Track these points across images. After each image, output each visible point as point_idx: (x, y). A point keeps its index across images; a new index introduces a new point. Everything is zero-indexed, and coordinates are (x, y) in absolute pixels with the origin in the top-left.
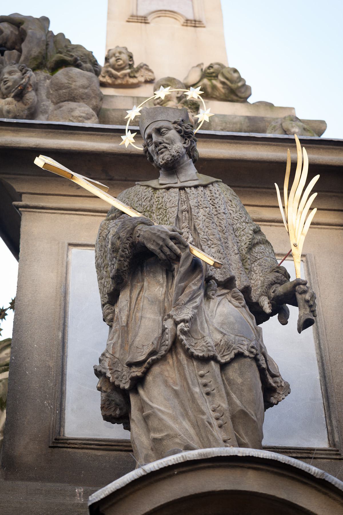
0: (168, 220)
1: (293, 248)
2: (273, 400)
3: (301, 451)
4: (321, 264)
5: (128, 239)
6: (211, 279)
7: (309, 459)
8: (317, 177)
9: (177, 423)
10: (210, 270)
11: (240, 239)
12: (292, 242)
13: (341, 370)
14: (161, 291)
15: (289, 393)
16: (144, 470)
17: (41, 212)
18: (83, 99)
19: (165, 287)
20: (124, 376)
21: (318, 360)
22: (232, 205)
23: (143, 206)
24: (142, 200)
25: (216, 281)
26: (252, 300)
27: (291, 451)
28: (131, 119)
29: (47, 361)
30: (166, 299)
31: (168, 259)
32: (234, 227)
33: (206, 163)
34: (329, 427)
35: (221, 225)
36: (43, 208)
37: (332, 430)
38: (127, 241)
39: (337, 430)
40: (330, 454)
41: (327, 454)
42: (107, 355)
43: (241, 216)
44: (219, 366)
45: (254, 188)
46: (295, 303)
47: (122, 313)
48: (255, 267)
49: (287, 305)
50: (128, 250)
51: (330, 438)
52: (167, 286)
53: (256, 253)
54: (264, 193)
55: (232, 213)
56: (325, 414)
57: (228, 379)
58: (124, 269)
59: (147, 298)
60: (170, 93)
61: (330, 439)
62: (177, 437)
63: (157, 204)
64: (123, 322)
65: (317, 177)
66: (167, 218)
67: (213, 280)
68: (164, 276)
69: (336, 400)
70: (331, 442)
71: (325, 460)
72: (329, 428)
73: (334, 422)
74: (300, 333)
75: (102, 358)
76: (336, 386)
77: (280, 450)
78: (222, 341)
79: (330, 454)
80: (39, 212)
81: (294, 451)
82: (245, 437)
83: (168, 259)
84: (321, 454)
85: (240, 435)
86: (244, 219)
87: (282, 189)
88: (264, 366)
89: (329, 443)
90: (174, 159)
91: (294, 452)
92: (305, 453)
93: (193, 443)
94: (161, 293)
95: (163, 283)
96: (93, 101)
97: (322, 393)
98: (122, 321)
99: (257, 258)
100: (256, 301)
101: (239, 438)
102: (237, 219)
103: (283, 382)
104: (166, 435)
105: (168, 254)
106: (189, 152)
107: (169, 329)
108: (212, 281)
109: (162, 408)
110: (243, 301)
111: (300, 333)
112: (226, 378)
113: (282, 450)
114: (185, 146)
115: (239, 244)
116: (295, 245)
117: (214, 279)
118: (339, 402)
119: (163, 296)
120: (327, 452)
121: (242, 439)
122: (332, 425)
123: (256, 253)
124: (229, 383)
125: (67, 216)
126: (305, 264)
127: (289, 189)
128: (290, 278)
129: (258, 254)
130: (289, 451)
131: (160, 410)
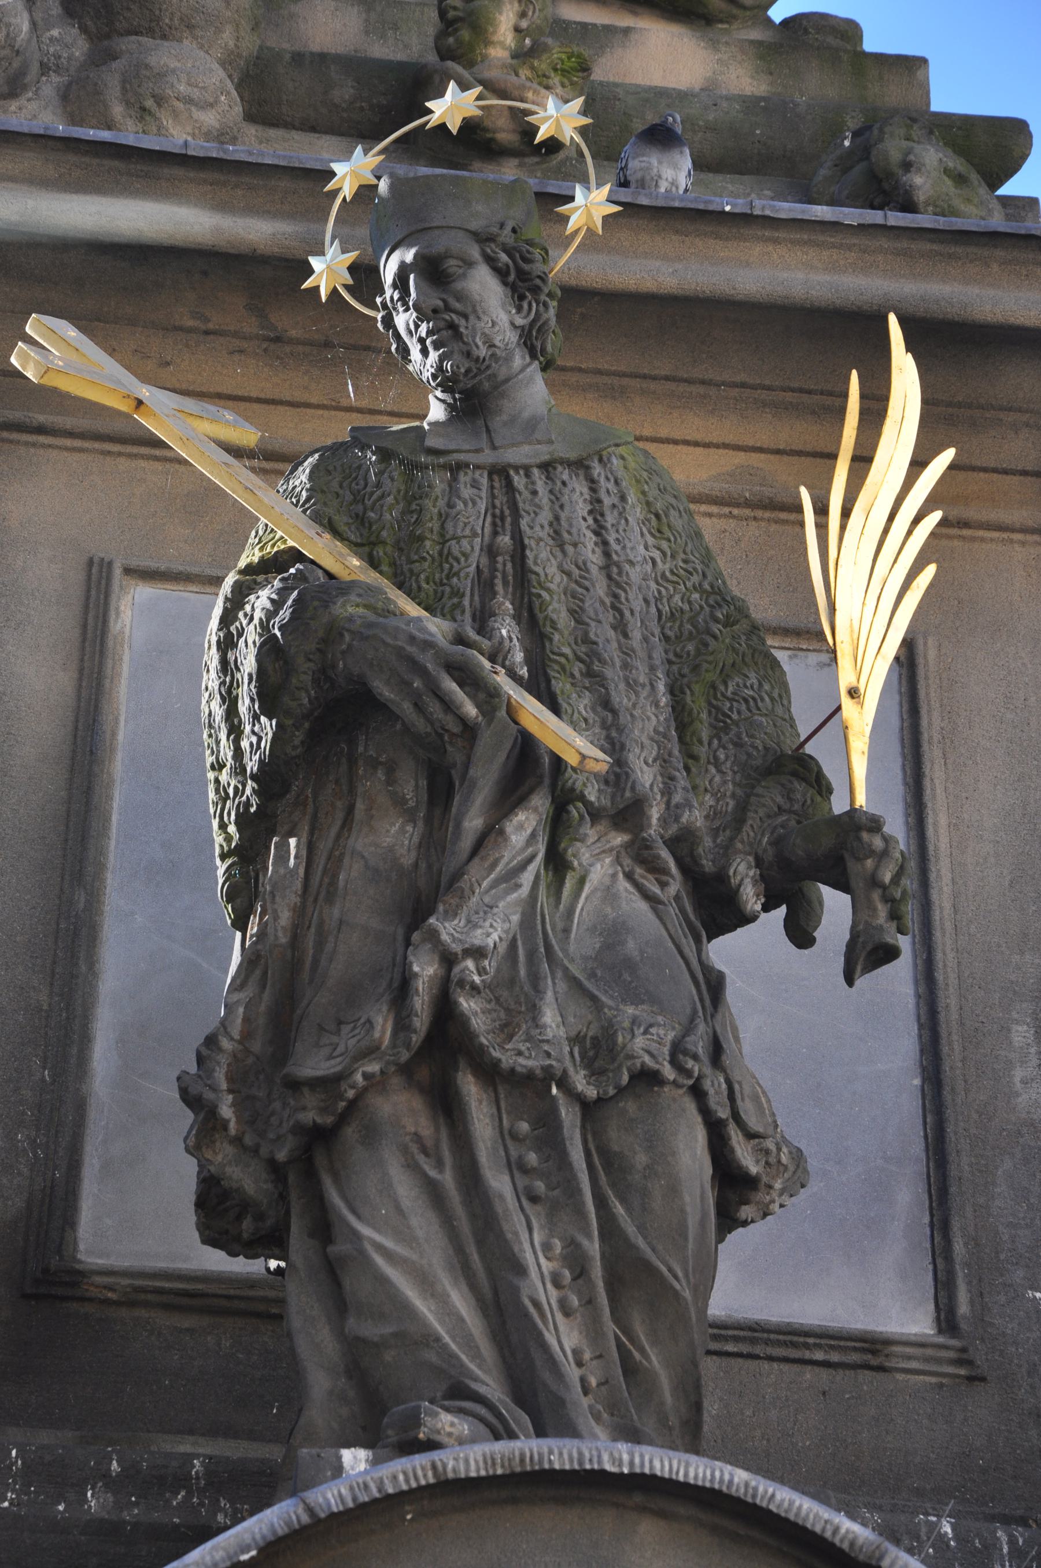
0: (445, 581)
1: (846, 702)
2: (746, 1212)
3: (842, 1343)
4: (960, 672)
5: (311, 657)
6: (568, 803)
7: (866, 1372)
8: (948, 455)
9: (432, 1295)
10: (569, 770)
11: (678, 649)
12: (844, 684)
13: (996, 1057)
14: (407, 835)
15: (803, 1186)
16: (310, 1510)
17: (34, 445)
18: (190, 27)
19: (420, 824)
20: (273, 1114)
21: (922, 1021)
22: (659, 531)
23: (367, 525)
24: (366, 501)
25: (587, 803)
26: (702, 866)
27: (811, 1341)
28: (344, 199)
29: (34, 987)
30: (423, 865)
31: (436, 732)
32: (660, 607)
33: (596, 299)
34: (939, 1261)
35: (618, 605)
36: (40, 430)
37: (951, 1273)
38: (306, 666)
39: (966, 1276)
40: (938, 1361)
41: (927, 1360)
42: (226, 1044)
43: (686, 570)
44: (577, 1109)
45: (754, 387)
46: (842, 885)
47: (277, 899)
48: (721, 750)
49: (821, 886)
50: (307, 691)
51: (943, 1301)
52: (429, 820)
53: (728, 698)
54: (787, 409)
55: (658, 560)
56: (932, 1215)
57: (605, 1153)
58: (294, 753)
59: (363, 857)
60: (479, 113)
61: (941, 1306)
62: (428, 1345)
63: (413, 520)
64: (280, 934)
65: (948, 455)
66: (444, 575)
67: (580, 805)
68: (420, 782)
69: (970, 1165)
70: (942, 1317)
71: (921, 1377)
72: (941, 1266)
73: (959, 1247)
74: (850, 980)
75: (205, 1052)
76: (975, 1116)
77: (772, 1336)
78: (591, 1026)
79: (938, 1361)
80: (27, 444)
81: (818, 1341)
82: (647, 1347)
83: (436, 732)
84: (909, 1358)
85: (632, 1340)
86: (695, 579)
87: (822, 510)
88: (723, 1113)
89: (938, 1319)
90: (479, 369)
91: (819, 1346)
92: (855, 1349)
93: (479, 1367)
94: (407, 842)
95: (417, 806)
96: (224, 36)
97: (926, 1137)
98: (279, 928)
99: (729, 717)
100: (713, 869)
101: (630, 1351)
102: (675, 579)
103: (785, 1150)
104: (395, 1335)
105: (435, 716)
106: (530, 339)
107: (426, 979)
108: (576, 808)
109: (389, 1244)
110: (672, 877)
111: (850, 980)
112: (597, 1148)
113: (781, 1337)
114: (520, 321)
115: (675, 668)
116: (853, 693)
117: (582, 798)
118: (981, 1171)
119: (413, 854)
120: (929, 1352)
121: (637, 1355)
122: (952, 1257)
123: (728, 698)
124: (608, 1165)
125: (123, 463)
126: (904, 671)
127: (846, 513)
128: (831, 793)
129: (735, 704)
130: (801, 1339)
131: (380, 1248)
